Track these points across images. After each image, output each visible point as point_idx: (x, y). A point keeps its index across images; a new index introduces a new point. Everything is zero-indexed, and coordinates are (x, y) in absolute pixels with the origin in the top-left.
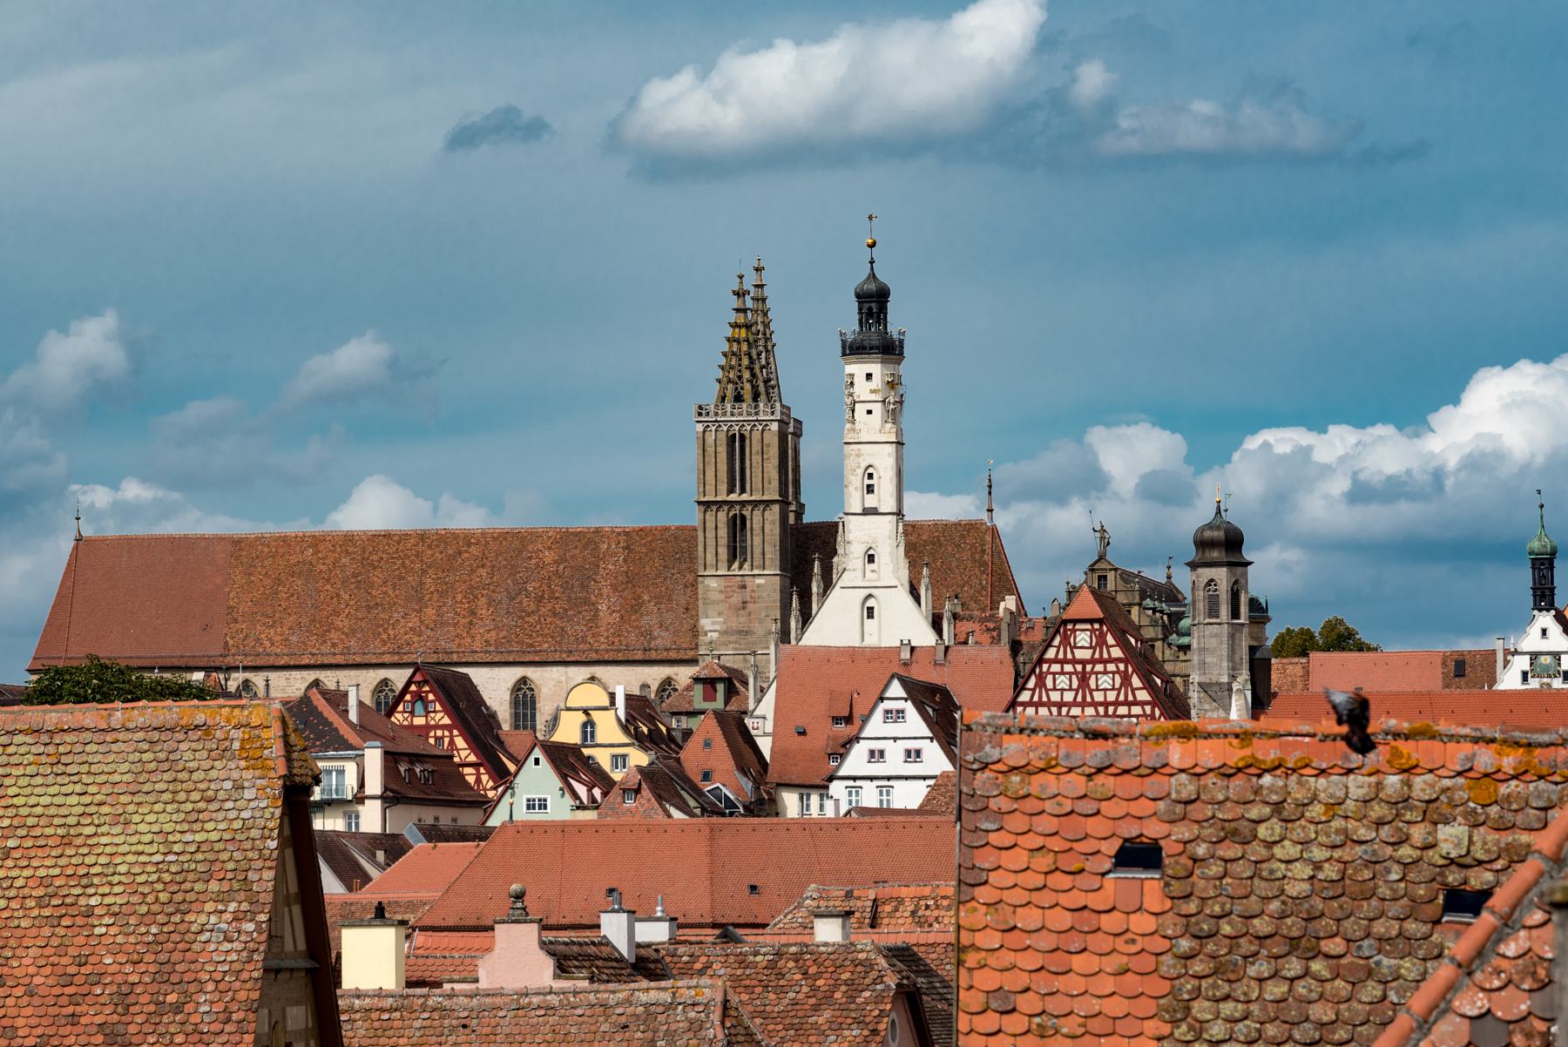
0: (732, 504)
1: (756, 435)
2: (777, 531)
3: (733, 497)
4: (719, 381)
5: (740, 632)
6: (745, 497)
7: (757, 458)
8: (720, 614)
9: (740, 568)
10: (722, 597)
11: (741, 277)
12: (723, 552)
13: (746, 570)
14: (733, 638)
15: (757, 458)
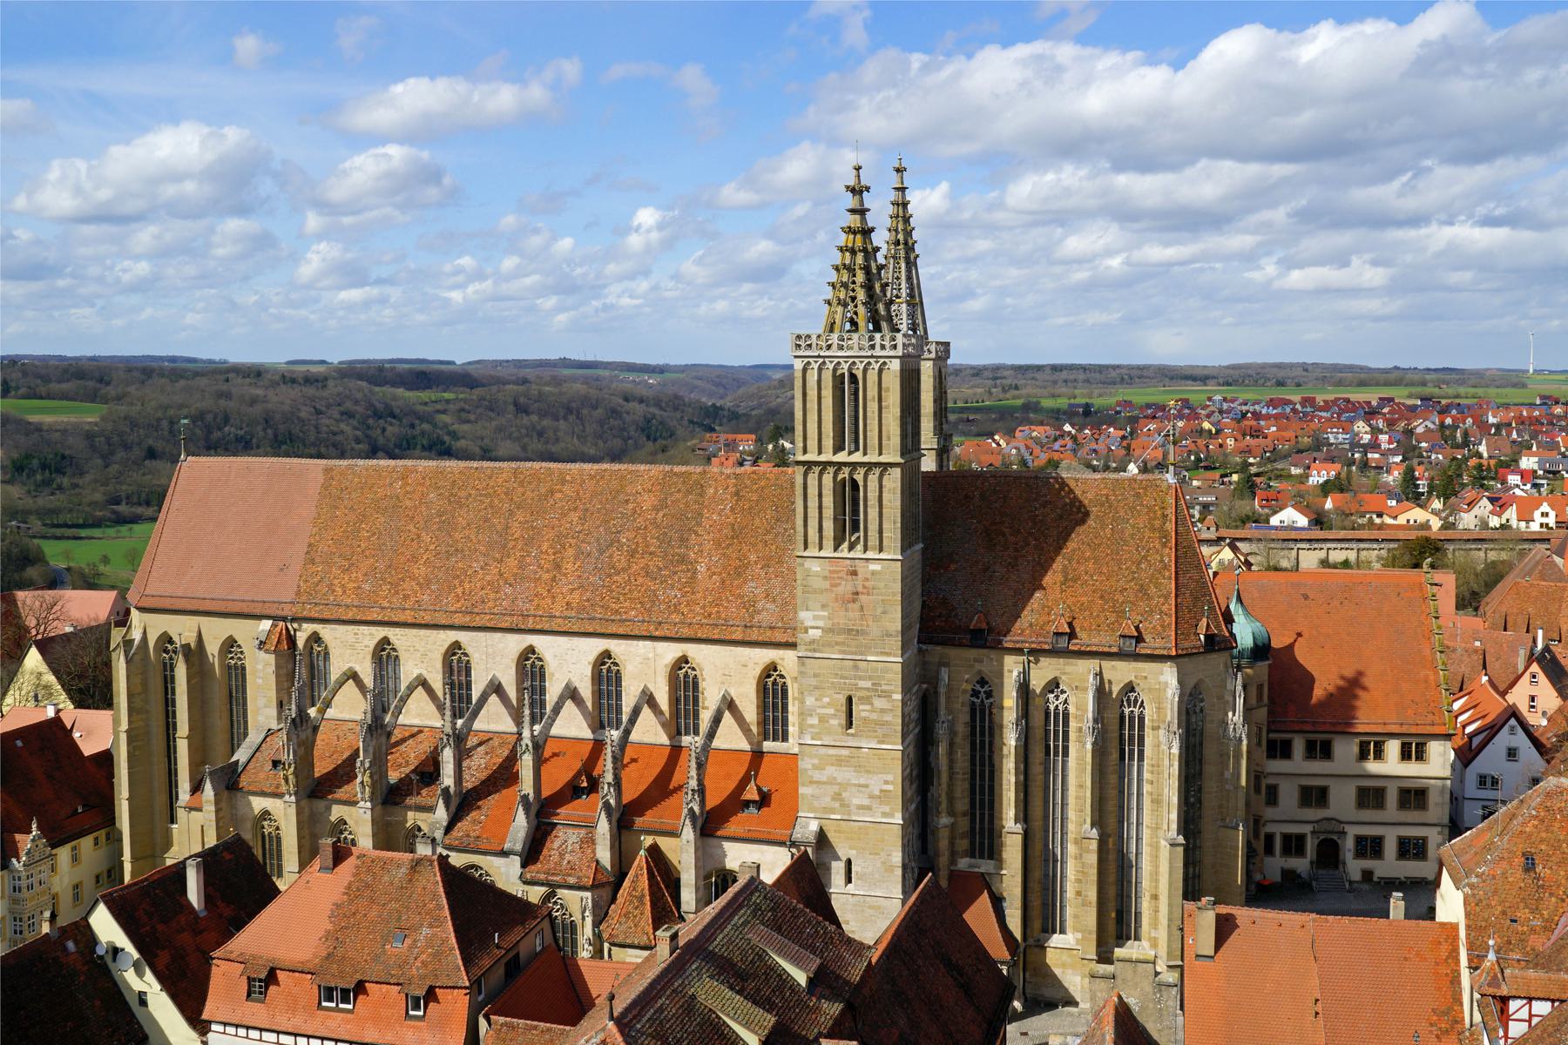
0: (840, 465)
1: (872, 376)
2: (898, 503)
3: (842, 457)
4: (829, 303)
5: (850, 631)
6: (857, 457)
7: (873, 407)
8: (824, 607)
9: (851, 548)
10: (827, 584)
11: (858, 169)
12: (829, 526)
13: (858, 552)
14: (840, 638)
15: (873, 407)
